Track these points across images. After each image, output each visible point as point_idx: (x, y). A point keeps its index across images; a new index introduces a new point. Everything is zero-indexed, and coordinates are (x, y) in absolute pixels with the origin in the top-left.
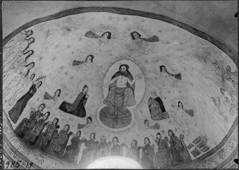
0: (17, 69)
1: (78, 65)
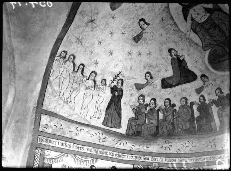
0: (79, 88)
1: (141, 38)
